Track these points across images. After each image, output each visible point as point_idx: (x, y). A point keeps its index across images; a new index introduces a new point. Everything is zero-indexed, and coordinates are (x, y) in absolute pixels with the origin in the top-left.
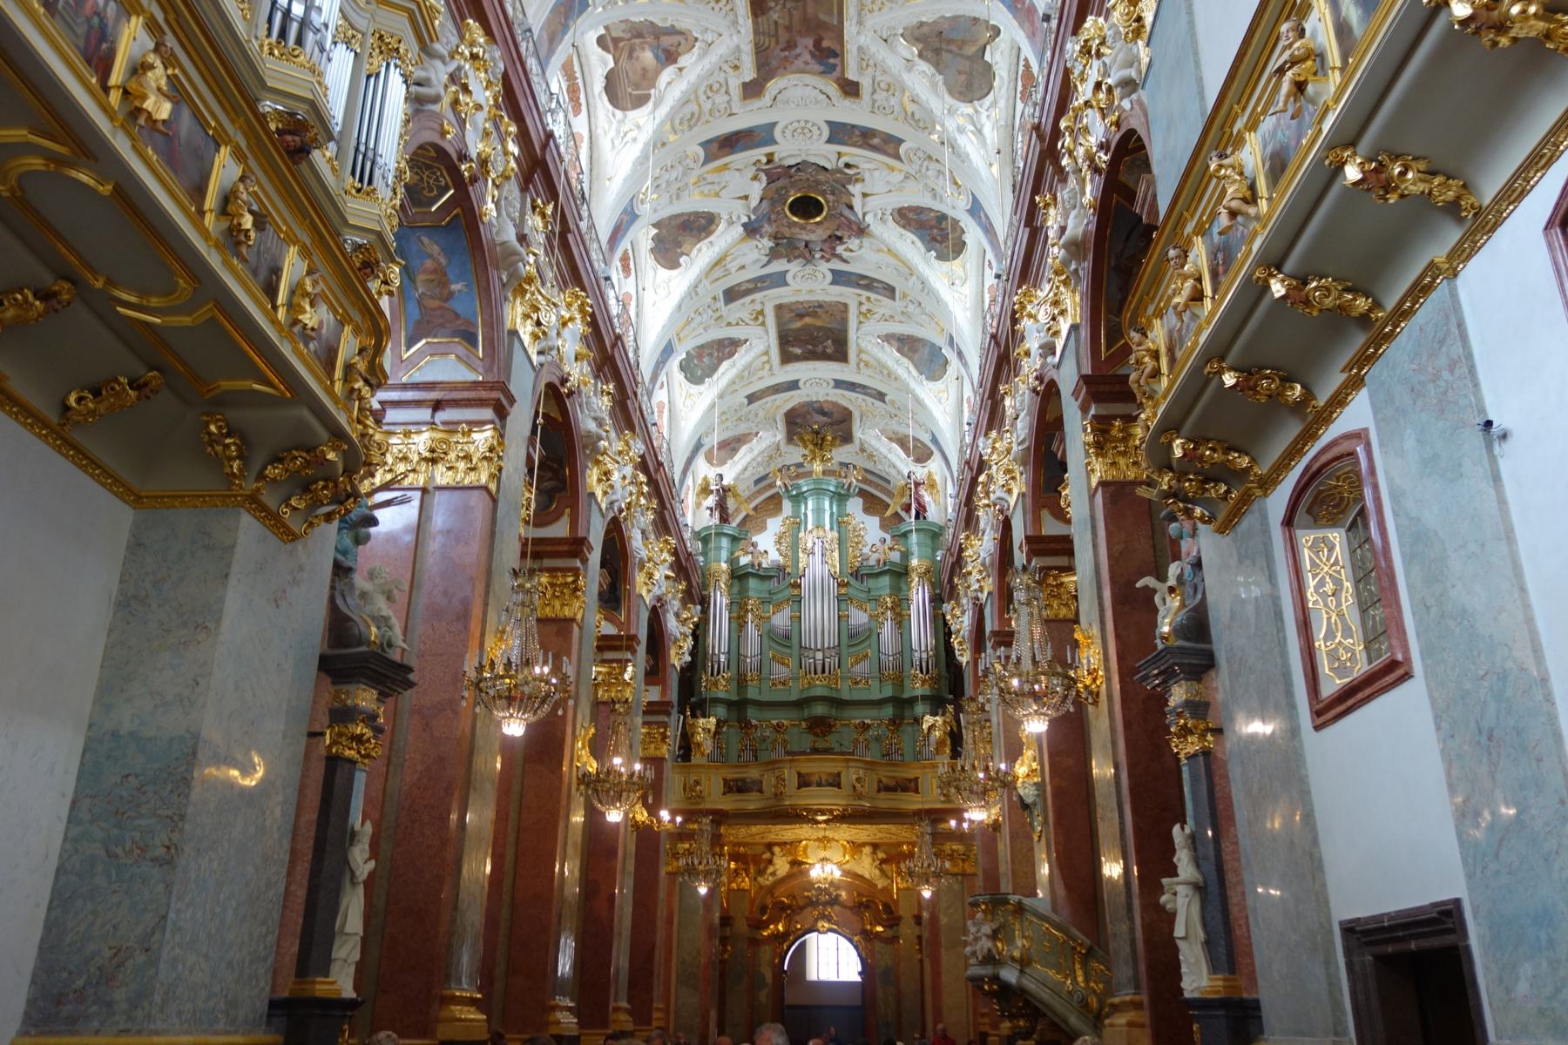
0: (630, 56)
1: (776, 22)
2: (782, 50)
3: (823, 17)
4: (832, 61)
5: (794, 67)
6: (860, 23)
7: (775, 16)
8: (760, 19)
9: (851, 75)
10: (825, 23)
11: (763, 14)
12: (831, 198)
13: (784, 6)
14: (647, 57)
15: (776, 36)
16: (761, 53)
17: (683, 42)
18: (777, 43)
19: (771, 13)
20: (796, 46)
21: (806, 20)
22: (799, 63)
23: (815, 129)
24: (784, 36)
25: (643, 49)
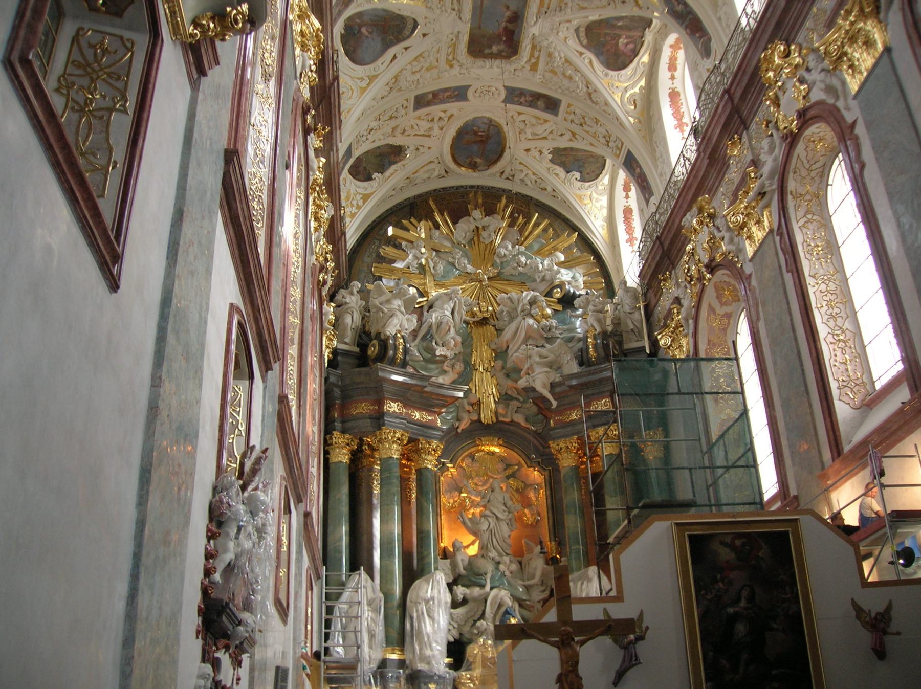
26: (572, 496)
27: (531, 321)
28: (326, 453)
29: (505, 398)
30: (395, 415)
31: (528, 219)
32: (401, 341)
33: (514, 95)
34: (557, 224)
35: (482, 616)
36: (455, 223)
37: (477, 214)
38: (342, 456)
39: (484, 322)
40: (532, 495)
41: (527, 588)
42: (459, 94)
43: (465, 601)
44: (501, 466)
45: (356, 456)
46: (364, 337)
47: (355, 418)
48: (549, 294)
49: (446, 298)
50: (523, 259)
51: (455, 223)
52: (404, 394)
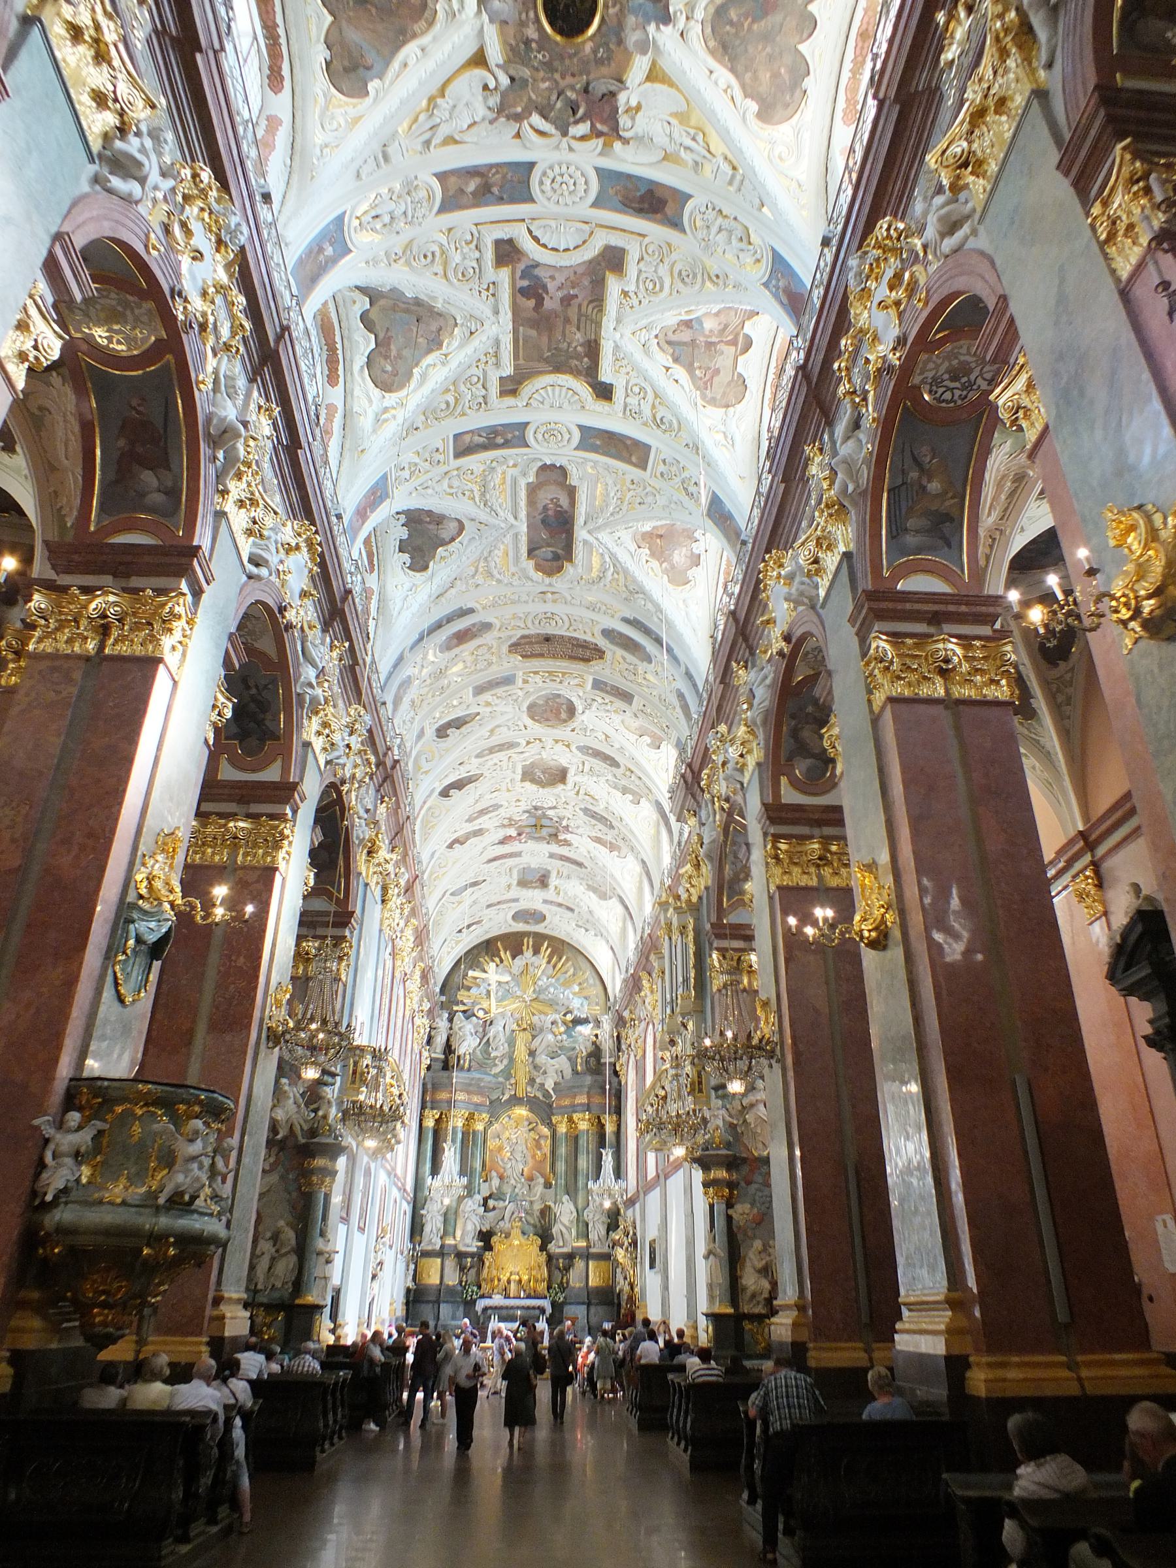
0: (726, 326)
1: (578, 329)
2: (576, 296)
3: (534, 333)
4: (525, 283)
5: (566, 274)
6: (497, 343)
7: (578, 336)
8: (593, 337)
9: (504, 276)
10: (532, 327)
11: (589, 342)
12: (531, 32)
13: (569, 344)
14: (709, 325)
15: (580, 315)
16: (598, 300)
17: (670, 334)
18: (580, 306)
19: (581, 340)
20: (562, 300)
21: (550, 329)
22: (560, 278)
23: (549, 193)
24: (573, 313)
25: (711, 331)
26: (562, 1150)
27: (550, 1037)
28: (421, 1120)
29: (532, 1081)
30: (461, 1101)
31: (561, 958)
32: (468, 1057)
33: (545, 902)
34: (580, 958)
35: (503, 1218)
36: (514, 957)
37: (528, 953)
38: (430, 1123)
39: (525, 1030)
40: (542, 1142)
41: (531, 1203)
42: (516, 900)
43: (494, 1208)
44: (526, 1123)
45: (438, 1121)
46: (449, 1049)
47: (438, 1102)
48: (565, 1015)
49: (500, 1018)
50: (552, 990)
51: (514, 957)
52: (467, 1089)
